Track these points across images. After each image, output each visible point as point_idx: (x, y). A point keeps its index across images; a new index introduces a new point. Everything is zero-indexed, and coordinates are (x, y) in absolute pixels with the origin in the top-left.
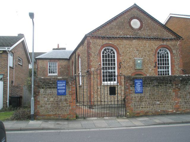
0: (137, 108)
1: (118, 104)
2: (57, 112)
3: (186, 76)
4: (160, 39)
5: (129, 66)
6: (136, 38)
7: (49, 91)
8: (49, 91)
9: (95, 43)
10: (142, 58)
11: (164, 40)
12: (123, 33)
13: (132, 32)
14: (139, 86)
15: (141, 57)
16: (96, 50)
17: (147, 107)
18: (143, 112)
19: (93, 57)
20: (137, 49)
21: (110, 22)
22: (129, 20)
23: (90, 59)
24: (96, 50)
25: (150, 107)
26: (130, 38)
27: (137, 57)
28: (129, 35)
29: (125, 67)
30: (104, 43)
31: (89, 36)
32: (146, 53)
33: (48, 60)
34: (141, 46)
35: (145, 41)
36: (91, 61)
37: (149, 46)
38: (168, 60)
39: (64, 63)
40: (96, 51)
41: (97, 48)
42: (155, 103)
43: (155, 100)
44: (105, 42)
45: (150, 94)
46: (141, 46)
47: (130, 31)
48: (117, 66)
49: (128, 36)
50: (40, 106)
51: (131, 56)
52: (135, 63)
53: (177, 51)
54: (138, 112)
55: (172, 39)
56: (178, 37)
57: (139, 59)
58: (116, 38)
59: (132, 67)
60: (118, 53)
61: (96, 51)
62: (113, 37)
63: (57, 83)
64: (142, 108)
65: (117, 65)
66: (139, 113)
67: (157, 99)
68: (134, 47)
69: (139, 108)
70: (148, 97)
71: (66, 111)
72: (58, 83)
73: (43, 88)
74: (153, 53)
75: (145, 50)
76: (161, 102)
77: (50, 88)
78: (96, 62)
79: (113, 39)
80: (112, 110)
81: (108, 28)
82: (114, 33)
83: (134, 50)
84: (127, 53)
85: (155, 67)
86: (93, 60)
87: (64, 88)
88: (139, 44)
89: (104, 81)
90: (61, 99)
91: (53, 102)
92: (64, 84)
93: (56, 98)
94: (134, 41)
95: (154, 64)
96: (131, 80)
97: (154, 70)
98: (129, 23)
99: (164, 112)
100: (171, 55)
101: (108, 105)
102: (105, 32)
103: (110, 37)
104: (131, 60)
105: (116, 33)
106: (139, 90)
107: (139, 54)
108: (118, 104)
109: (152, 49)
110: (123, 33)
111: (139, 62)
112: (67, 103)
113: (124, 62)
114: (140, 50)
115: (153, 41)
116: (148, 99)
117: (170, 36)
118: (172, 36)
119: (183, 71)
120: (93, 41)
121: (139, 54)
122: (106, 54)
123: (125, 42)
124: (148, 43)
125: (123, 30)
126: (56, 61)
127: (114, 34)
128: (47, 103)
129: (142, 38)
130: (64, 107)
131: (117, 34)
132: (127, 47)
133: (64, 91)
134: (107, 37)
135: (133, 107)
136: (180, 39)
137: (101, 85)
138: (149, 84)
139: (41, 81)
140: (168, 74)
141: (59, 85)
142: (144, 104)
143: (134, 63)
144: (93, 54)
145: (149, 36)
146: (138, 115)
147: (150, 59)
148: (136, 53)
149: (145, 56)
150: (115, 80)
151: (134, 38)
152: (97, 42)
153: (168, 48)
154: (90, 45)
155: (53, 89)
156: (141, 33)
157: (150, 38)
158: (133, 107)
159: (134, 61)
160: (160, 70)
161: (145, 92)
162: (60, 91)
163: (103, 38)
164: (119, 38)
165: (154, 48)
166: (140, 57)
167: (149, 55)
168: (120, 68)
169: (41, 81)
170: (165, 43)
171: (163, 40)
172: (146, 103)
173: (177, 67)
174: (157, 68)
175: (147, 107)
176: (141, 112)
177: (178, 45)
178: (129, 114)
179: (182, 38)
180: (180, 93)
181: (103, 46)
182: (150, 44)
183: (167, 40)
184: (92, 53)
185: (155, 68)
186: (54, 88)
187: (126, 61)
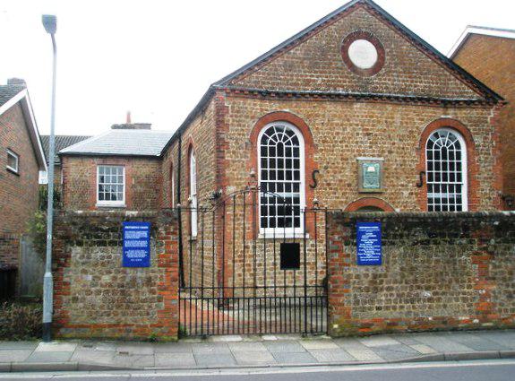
0: (363, 309)
1: (305, 297)
2: (123, 319)
3: (511, 214)
4: (435, 101)
5: (341, 181)
6: (363, 96)
7: (100, 254)
8: (100, 254)
9: (238, 112)
10: (382, 159)
11: (449, 106)
12: (323, 81)
14: (371, 241)
15: (379, 156)
16: (243, 130)
17: (394, 308)
18: (380, 320)
19: (234, 152)
21: (286, 47)
22: (344, 42)
23: (223, 158)
24: (243, 130)
25: (402, 307)
26: (347, 96)
27: (365, 156)
28: (343, 86)
29: (329, 184)
30: (267, 110)
31: (221, 90)
32: (394, 144)
33: (97, 161)
34: (379, 122)
35: (390, 108)
36: (227, 164)
37: (402, 123)
38: (459, 165)
39: (145, 169)
40: (243, 135)
41: (244, 126)
42: (417, 295)
43: (419, 288)
44: (272, 106)
45: (402, 269)
46: (379, 122)
47: (347, 77)
50: (71, 297)
53: (486, 138)
54: (367, 320)
55: (473, 102)
56: (490, 98)
57: (372, 161)
58: (303, 95)
59: (349, 185)
60: (308, 141)
61: (243, 135)
62: (294, 94)
63: (123, 231)
64: (378, 308)
65: (306, 178)
66: (368, 326)
67: (423, 282)
68: (357, 125)
69: (370, 309)
70: (398, 277)
71: (148, 314)
72: (127, 230)
73: (80, 244)
74: (414, 145)
77: (102, 243)
78: (243, 166)
79: (294, 99)
80: (288, 315)
82: (298, 80)
83: (358, 134)
84: (336, 142)
85: (419, 186)
86: (234, 162)
87: (143, 244)
88: (373, 117)
89: (264, 225)
90: (134, 279)
91: (110, 285)
92: (145, 234)
93: (120, 276)
94: (358, 105)
95: (418, 176)
96: (346, 225)
98: (345, 50)
99: (445, 323)
100: (468, 151)
101: (276, 297)
102: (271, 79)
103: (286, 94)
105: (304, 80)
106: (369, 256)
108: (305, 297)
110: (323, 81)
111: (371, 169)
112: (153, 292)
113: (326, 168)
115: (414, 108)
116: (395, 282)
118: (471, 94)
119: (503, 198)
120: (234, 103)
122: (271, 143)
123: (331, 108)
124: (398, 114)
125: (324, 72)
126: (122, 161)
127: (296, 84)
128: (93, 289)
129: (381, 97)
130: (144, 301)
131: (307, 83)
132: (337, 124)
133: (142, 254)
134: (277, 94)
135: (352, 306)
136: (495, 103)
137: (255, 237)
138: (401, 236)
139: (74, 224)
140: (459, 208)
141: (128, 235)
142: (383, 298)
143: (354, 172)
144: (232, 143)
145: (403, 90)
146: (365, 330)
148: (362, 142)
149: (390, 152)
150: (297, 224)
151: (358, 98)
152: (246, 108)
153: (461, 128)
154: (223, 115)
155: (110, 248)
156: (383, 84)
157: (404, 99)
158: (352, 306)
159: (357, 168)
160: (433, 195)
161: (388, 262)
162: (130, 254)
163: (265, 95)
164: (312, 95)
165: (417, 128)
166: (373, 156)
167: (403, 148)
168: (313, 187)
169: (74, 224)
171: (446, 104)
172: (391, 295)
173: (485, 187)
174: (424, 188)
175: (394, 308)
176: (376, 321)
177: (489, 120)
179: (502, 99)
180: (495, 267)
181: (264, 120)
182: (407, 115)
183: (456, 104)
186: (113, 243)
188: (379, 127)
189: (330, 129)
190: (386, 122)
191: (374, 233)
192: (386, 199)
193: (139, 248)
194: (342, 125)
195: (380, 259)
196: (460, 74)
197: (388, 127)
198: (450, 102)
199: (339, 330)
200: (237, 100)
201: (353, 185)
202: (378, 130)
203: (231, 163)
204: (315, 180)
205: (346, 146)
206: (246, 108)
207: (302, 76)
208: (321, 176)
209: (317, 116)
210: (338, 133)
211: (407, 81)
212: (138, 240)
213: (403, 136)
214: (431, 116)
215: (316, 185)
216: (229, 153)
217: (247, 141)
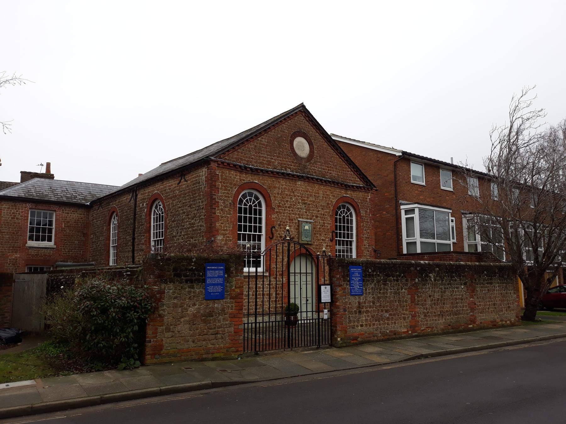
3: (425, 263)
4: (341, 184)
9: (226, 179)
12: (278, 163)
13: (296, 163)
15: (311, 219)
16: (228, 193)
18: (363, 334)
19: (222, 210)
20: (304, 200)
22: (291, 137)
24: (228, 193)
27: (303, 218)
31: (215, 161)
32: (319, 211)
33: (29, 205)
34: (311, 195)
35: (317, 186)
37: (323, 197)
38: (260, 219)
39: (74, 216)
40: (229, 197)
41: (229, 191)
42: (381, 316)
43: (382, 311)
44: (248, 178)
48: (266, 234)
49: (289, 171)
51: (293, 214)
52: (300, 230)
53: (366, 212)
55: (360, 187)
56: (369, 185)
57: (307, 222)
58: (267, 172)
60: (268, 205)
61: (229, 197)
62: (262, 171)
63: (205, 270)
66: (356, 339)
69: (357, 326)
72: (209, 270)
75: (316, 205)
76: (390, 315)
81: (252, 148)
83: (299, 203)
84: (286, 207)
85: (331, 241)
87: (220, 280)
95: (331, 234)
97: (330, 246)
99: (395, 334)
101: (307, 320)
104: (292, 223)
105: (267, 161)
107: (306, 213)
109: (328, 204)
111: (307, 227)
113: (279, 225)
114: (309, 204)
116: (370, 307)
117: (357, 181)
118: (354, 180)
119: (375, 251)
120: (223, 173)
121: (306, 213)
122: (245, 205)
123: (283, 183)
124: (321, 191)
126: (53, 207)
129: (312, 178)
132: (287, 195)
133: (219, 289)
134: (251, 169)
140: (351, 256)
141: (209, 274)
143: (297, 229)
144: (221, 202)
146: (355, 342)
147: (324, 223)
148: (301, 208)
149: (317, 217)
151: (300, 178)
153: (354, 204)
154: (216, 181)
156: (315, 169)
157: (325, 181)
159: (298, 226)
160: (338, 247)
162: (210, 289)
163: (244, 169)
164: (272, 172)
165: (331, 201)
166: (307, 219)
168: (271, 238)
170: (349, 194)
171: (347, 187)
172: (368, 316)
177: (368, 199)
178: (341, 339)
179: (375, 187)
180: (418, 297)
181: (242, 187)
183: (353, 188)
184: (220, 201)
185: (331, 244)
186: (198, 281)
187: (283, 225)
188: (311, 199)
189: (283, 198)
190: (315, 196)
191: (359, 273)
192: (314, 248)
193: (217, 285)
194: (290, 195)
195: (362, 291)
196: (353, 168)
197: (315, 199)
198: (349, 186)
199: (341, 342)
200: (224, 170)
201: (295, 238)
202: (310, 201)
203: (220, 218)
204: (272, 234)
205: (292, 211)
206: (231, 177)
207: (265, 157)
208: (277, 231)
209: (275, 187)
210: (287, 201)
211: (326, 169)
212: (216, 277)
213: (324, 206)
214: (338, 194)
215: (273, 236)
216: (218, 210)
217: (230, 202)
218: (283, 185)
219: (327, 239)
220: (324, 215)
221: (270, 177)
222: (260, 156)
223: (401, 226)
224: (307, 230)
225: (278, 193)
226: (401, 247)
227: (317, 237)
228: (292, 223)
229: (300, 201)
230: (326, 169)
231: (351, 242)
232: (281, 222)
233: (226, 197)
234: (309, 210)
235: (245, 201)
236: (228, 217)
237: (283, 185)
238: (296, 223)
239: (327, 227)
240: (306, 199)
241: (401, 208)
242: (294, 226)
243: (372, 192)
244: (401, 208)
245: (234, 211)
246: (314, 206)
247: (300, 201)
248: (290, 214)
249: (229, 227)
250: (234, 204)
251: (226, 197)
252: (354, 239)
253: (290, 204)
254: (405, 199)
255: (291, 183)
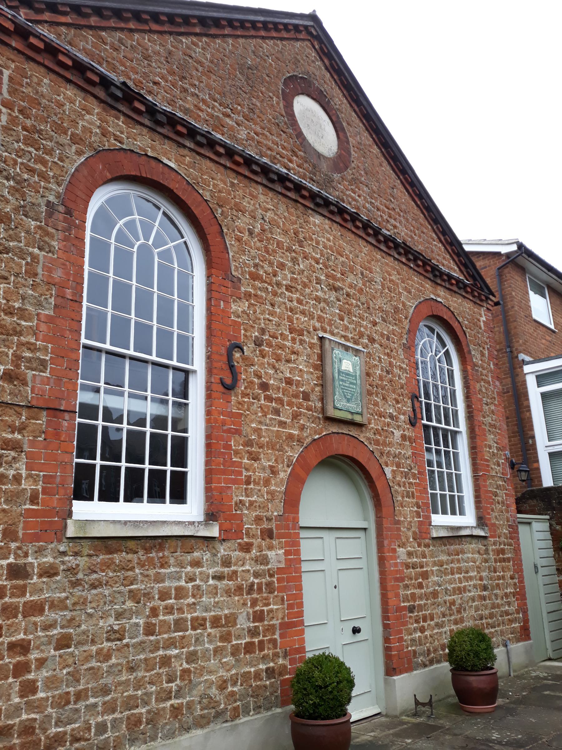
5: (289, 382)
20: (334, 278)
29: (264, 387)
32: (375, 324)
34: (352, 270)
41: (50, 152)
48: (210, 371)
51: (303, 313)
52: (328, 369)
59: (306, 396)
61: (43, 176)
65: (209, 358)
83: (319, 282)
84: (279, 284)
85: (413, 424)
94: (317, 220)
95: (409, 402)
97: (410, 439)
114: (348, 295)
119: (512, 466)
121: (342, 319)
132: (279, 244)
143: (316, 367)
147: (390, 363)
148: (325, 301)
149: (372, 340)
159: (321, 357)
165: (404, 304)
166: (345, 337)
168: (229, 388)
177: (482, 324)
187: (269, 345)
189: (267, 252)
190: (362, 274)
197: (364, 285)
198: (442, 274)
201: (313, 397)
202: (351, 286)
209: (239, 208)
210: (282, 266)
217: (52, 198)
218: (267, 210)
219: (402, 417)
220: (388, 339)
221: (222, 169)
222: (185, 90)
223: (530, 414)
224: (347, 374)
225: (251, 233)
226: (535, 465)
227: (376, 404)
228: (302, 342)
229: (323, 278)
230: (384, 212)
231: (455, 434)
232: (263, 331)
233: (32, 171)
234: (349, 313)
235: (121, 222)
236: (35, 258)
237: (267, 210)
238: (312, 346)
239: (400, 378)
240: (339, 275)
241: (525, 372)
242: (308, 356)
243: (488, 306)
244: (525, 372)
245: (66, 239)
246: (363, 304)
247: (323, 278)
248: (291, 310)
249: (39, 304)
250: (69, 212)
251: (32, 171)
252: (463, 427)
253: (292, 279)
254: (529, 352)
255: (292, 210)
